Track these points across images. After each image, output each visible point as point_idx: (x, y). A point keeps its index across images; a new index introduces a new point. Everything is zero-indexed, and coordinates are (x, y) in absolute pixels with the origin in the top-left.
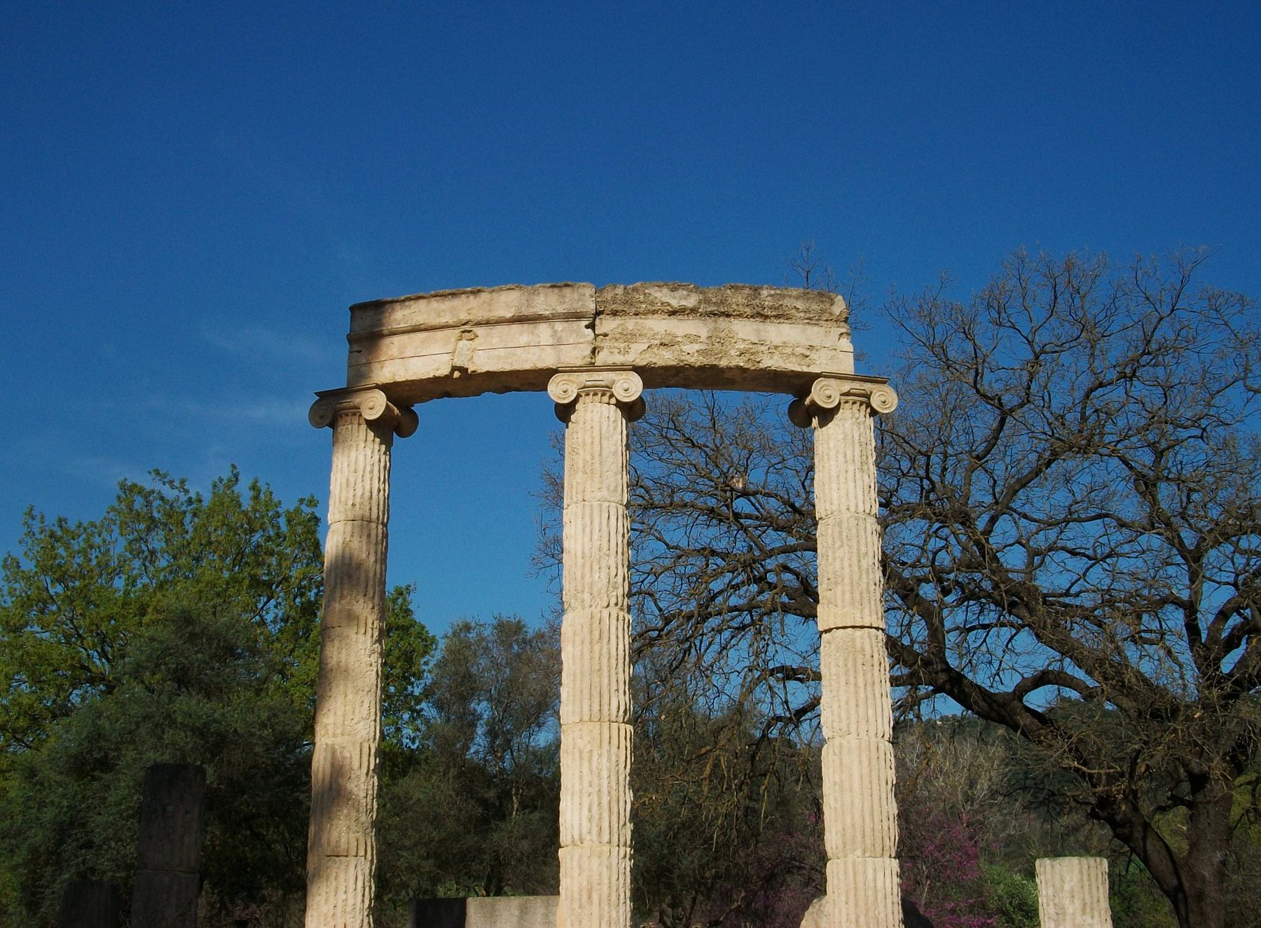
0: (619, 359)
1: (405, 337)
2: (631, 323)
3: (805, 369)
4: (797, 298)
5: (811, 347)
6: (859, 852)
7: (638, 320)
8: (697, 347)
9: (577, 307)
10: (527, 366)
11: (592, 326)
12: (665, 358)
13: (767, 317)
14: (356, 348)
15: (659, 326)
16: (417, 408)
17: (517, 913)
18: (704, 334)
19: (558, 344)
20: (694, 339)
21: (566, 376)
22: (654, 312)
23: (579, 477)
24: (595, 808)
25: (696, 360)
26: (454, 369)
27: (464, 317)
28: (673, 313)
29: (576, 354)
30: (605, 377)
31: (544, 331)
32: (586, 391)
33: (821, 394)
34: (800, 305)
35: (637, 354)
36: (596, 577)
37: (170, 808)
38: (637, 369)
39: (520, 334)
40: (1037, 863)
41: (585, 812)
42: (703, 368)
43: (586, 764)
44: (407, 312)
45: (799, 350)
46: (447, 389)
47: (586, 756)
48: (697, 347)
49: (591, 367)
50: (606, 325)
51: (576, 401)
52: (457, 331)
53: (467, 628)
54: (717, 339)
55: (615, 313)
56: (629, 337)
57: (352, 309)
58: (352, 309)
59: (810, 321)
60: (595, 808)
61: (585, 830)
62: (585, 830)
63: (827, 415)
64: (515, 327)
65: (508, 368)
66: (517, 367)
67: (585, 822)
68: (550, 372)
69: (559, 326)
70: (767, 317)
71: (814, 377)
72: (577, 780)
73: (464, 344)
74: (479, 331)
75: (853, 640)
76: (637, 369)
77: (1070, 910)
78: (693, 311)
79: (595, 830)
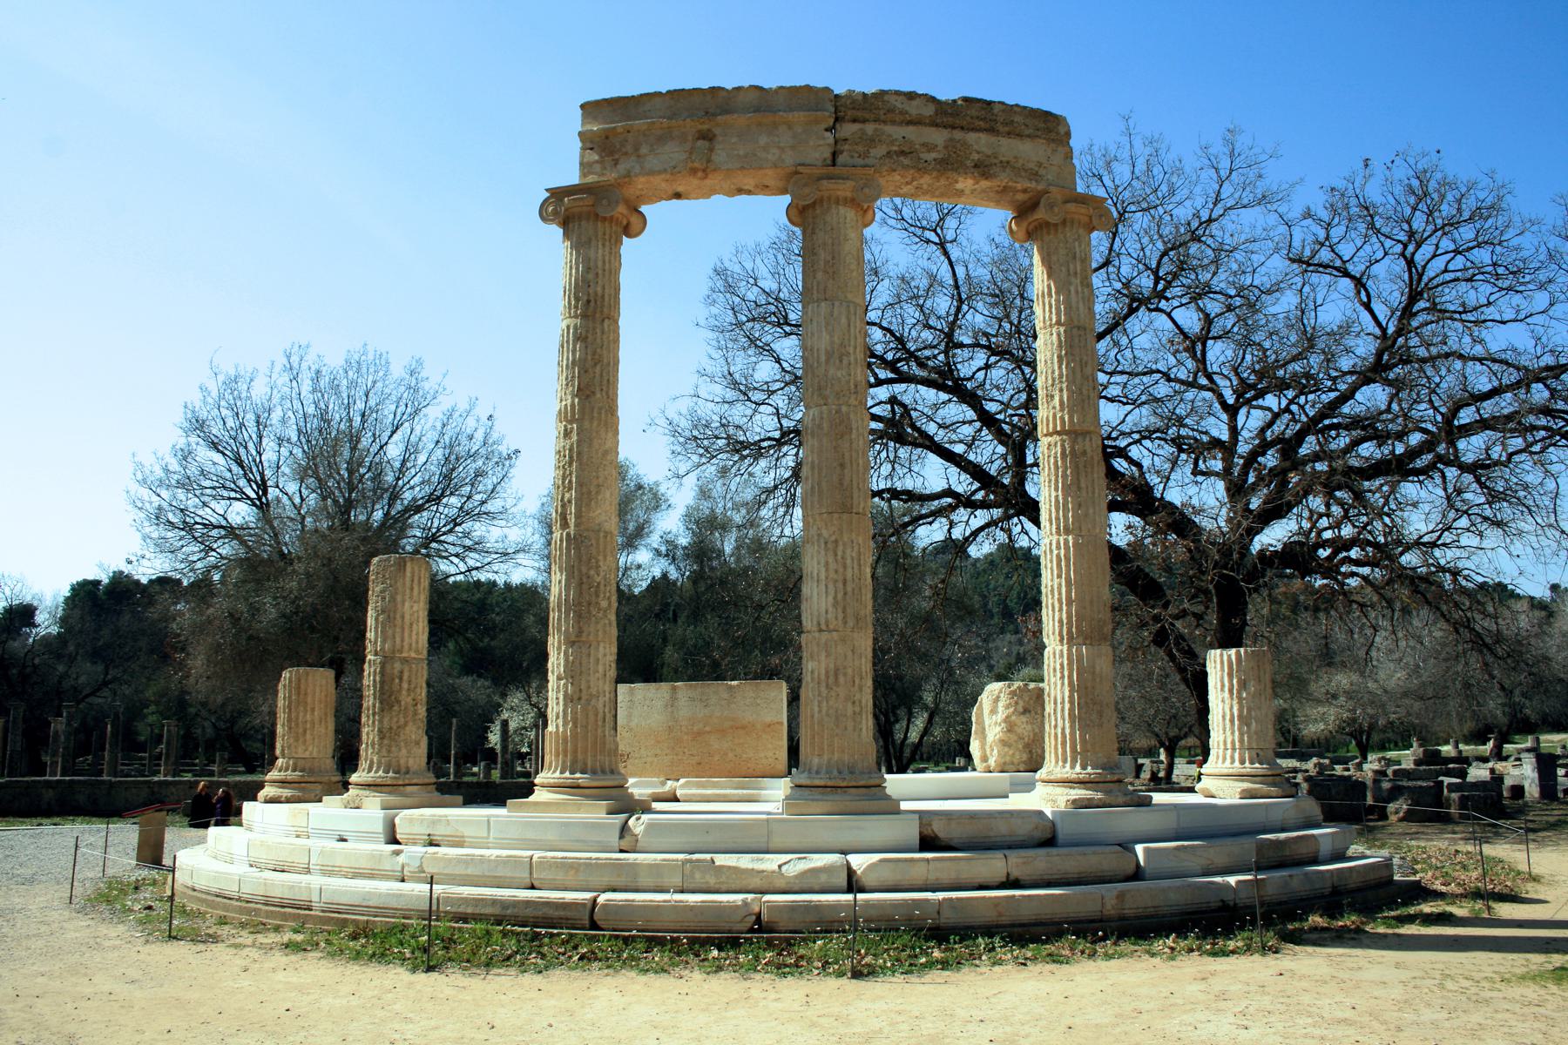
5: (1040, 165)
8: (934, 155)
16: (644, 209)
41: (830, 598)
43: (831, 553)
45: (1031, 165)
46: (680, 189)
48: (934, 155)
56: (872, 141)
57: (582, 106)
58: (582, 106)
60: (840, 596)
72: (823, 570)
79: (840, 616)
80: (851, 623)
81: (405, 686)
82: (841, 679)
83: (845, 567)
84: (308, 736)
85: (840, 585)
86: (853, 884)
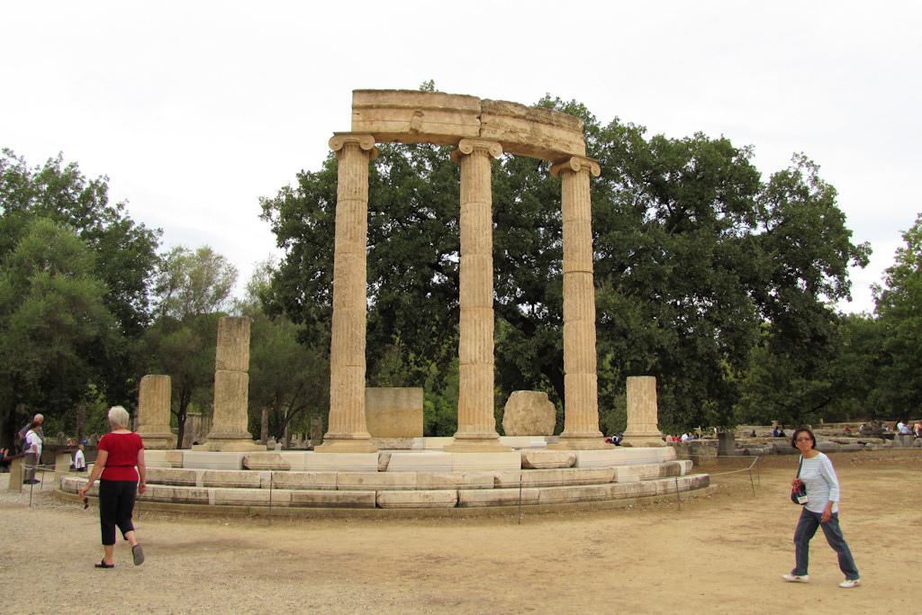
0: (493, 136)
1: (385, 111)
2: (497, 119)
3: (567, 152)
4: (565, 118)
5: (570, 142)
6: (584, 370)
7: (501, 118)
8: (525, 135)
9: (473, 108)
10: (449, 133)
11: (479, 118)
12: (512, 138)
13: (553, 125)
14: (356, 112)
15: (509, 122)
17: (393, 395)
18: (529, 129)
19: (463, 125)
20: (524, 131)
21: (467, 141)
22: (507, 115)
23: (473, 190)
24: (482, 346)
25: (525, 141)
26: (411, 129)
27: (417, 104)
28: (515, 117)
29: (472, 130)
30: (487, 144)
31: (457, 118)
32: (476, 150)
33: (573, 163)
34: (566, 122)
35: (499, 135)
36: (482, 239)
37: (238, 339)
38: (500, 142)
39: (446, 118)
40: (629, 378)
41: (477, 349)
42: (527, 145)
43: (477, 328)
44: (385, 97)
45: (566, 143)
47: (477, 322)
48: (525, 135)
49: (479, 138)
50: (487, 119)
51: (470, 155)
52: (413, 111)
53: (180, 250)
54: (534, 133)
55: (490, 113)
56: (498, 126)
57: (354, 92)
58: (354, 92)
59: (570, 130)
60: (482, 346)
61: (477, 357)
62: (477, 357)
63: (572, 172)
64: (443, 114)
65: (439, 133)
66: (444, 133)
67: (478, 353)
68: (460, 138)
69: (464, 116)
70: (553, 125)
71: (572, 155)
72: (473, 334)
73: (415, 117)
74: (424, 112)
75: (583, 277)
76: (500, 142)
77: (644, 398)
78: (524, 118)
80: (487, 361)
81: (241, 386)
82: (482, 388)
83: (484, 332)
84: (160, 414)
85: (482, 342)
86: (497, 485)
